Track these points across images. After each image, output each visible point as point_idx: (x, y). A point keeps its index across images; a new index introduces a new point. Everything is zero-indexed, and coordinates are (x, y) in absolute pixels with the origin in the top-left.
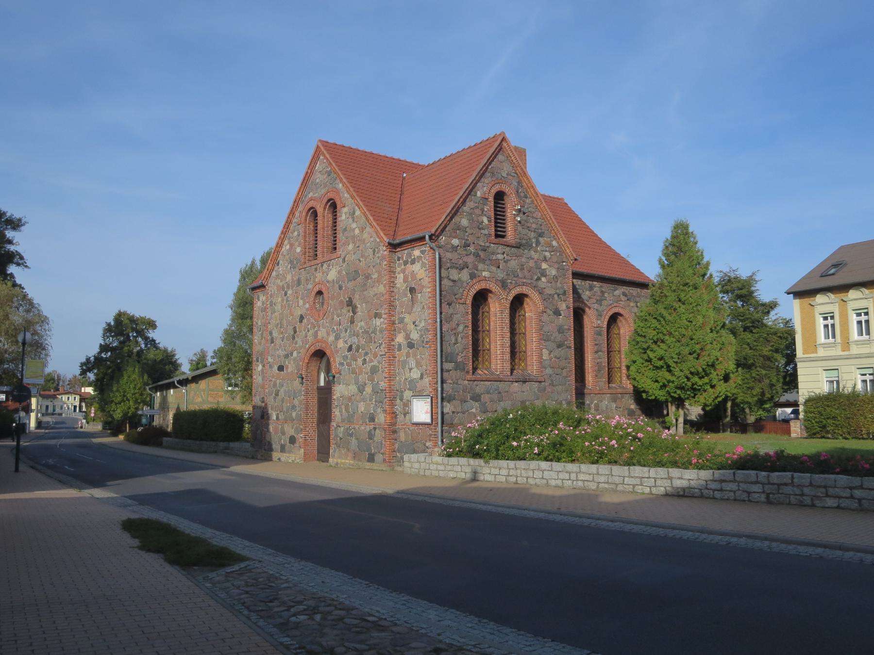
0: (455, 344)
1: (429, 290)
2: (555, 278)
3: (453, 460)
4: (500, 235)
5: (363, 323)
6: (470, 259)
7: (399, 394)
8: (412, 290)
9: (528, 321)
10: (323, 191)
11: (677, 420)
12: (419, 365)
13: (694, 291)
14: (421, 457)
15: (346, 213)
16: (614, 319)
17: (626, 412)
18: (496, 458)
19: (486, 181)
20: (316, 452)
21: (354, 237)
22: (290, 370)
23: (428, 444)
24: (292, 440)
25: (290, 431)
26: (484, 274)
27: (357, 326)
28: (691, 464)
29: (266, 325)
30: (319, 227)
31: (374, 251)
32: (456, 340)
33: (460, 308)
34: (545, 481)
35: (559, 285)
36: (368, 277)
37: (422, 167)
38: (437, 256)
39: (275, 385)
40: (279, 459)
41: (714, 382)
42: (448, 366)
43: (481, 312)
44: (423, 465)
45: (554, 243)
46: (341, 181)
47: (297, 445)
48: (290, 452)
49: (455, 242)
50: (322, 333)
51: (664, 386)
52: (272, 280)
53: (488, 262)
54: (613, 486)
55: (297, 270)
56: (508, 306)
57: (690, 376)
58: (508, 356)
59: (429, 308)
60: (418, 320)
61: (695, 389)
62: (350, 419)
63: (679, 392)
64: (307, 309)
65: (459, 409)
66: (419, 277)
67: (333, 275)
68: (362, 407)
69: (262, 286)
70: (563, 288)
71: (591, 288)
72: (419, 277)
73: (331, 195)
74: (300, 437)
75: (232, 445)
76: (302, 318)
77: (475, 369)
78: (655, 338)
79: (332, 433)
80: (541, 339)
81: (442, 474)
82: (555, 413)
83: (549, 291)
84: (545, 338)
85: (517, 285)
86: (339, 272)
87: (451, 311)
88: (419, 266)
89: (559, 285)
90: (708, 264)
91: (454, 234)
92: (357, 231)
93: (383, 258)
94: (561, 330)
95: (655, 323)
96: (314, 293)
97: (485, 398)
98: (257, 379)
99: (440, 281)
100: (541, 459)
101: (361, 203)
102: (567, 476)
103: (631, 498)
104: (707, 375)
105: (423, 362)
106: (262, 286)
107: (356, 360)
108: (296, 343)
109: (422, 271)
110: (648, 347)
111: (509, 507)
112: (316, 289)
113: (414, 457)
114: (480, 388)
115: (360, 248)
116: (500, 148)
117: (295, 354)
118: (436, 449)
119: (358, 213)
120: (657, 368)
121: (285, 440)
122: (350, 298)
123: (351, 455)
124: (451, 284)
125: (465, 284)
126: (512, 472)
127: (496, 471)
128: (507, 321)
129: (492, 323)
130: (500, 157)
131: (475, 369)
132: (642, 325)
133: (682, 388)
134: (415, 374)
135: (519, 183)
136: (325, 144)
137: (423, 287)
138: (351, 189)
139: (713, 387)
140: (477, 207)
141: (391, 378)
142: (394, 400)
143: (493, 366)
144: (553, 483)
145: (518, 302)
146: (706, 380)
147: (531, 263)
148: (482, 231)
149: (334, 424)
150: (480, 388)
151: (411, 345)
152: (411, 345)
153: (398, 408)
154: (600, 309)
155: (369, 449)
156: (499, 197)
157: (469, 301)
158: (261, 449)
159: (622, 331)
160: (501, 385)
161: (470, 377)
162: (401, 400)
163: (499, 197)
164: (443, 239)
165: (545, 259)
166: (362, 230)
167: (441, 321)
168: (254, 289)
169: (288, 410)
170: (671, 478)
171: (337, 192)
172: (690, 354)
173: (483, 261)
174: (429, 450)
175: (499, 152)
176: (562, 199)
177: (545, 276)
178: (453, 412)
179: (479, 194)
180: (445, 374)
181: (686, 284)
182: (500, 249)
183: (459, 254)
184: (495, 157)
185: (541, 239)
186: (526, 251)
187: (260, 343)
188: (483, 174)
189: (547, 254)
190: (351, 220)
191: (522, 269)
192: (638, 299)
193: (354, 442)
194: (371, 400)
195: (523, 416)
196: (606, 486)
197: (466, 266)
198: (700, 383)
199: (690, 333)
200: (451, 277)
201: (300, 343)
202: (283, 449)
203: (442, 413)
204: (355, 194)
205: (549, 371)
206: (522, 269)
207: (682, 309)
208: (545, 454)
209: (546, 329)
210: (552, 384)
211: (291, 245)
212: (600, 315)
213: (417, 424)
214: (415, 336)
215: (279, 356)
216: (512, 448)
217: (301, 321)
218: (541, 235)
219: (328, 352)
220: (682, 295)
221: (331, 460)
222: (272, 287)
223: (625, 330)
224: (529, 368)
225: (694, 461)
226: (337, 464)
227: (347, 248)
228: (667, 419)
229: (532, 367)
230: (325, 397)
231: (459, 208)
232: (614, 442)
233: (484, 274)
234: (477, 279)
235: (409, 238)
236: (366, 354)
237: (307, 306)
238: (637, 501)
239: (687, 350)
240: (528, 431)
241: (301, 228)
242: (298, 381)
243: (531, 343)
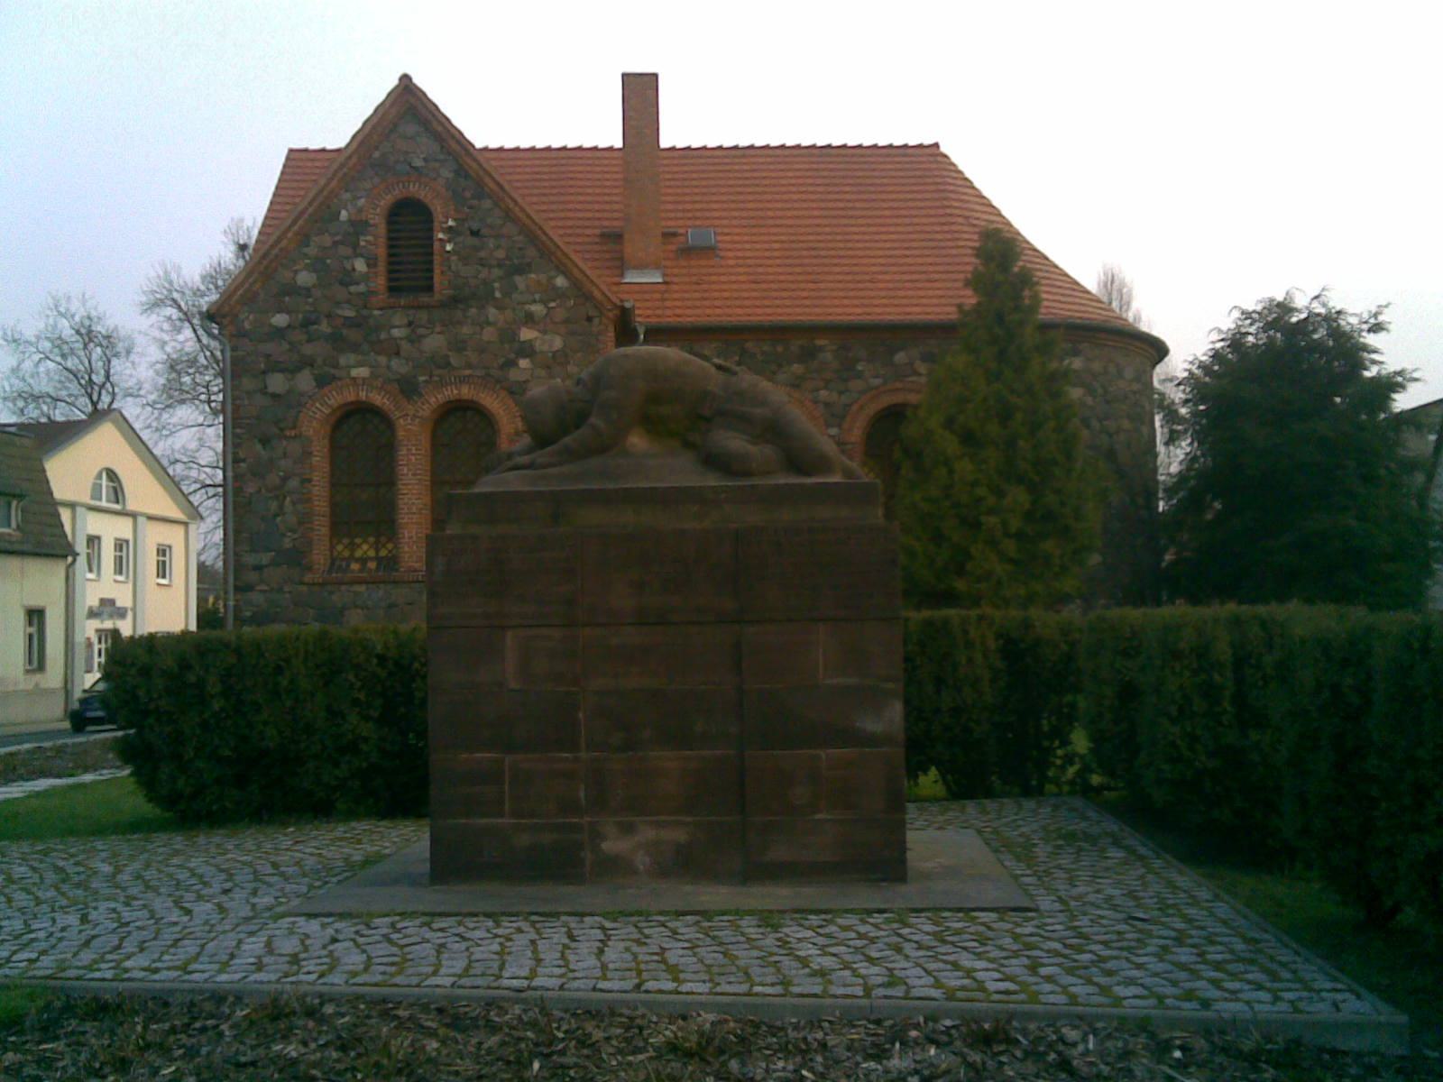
0: (276, 515)
2: (560, 358)
26: (355, 372)
32: (281, 507)
45: (560, 281)
49: (280, 320)
53: (365, 347)
147: (489, 334)
148: (353, 289)
165: (530, 319)
173: (355, 348)
179: (344, 215)
182: (399, 318)
183: (290, 343)
186: (473, 311)
189: (537, 309)
197: (309, 363)
200: (270, 390)
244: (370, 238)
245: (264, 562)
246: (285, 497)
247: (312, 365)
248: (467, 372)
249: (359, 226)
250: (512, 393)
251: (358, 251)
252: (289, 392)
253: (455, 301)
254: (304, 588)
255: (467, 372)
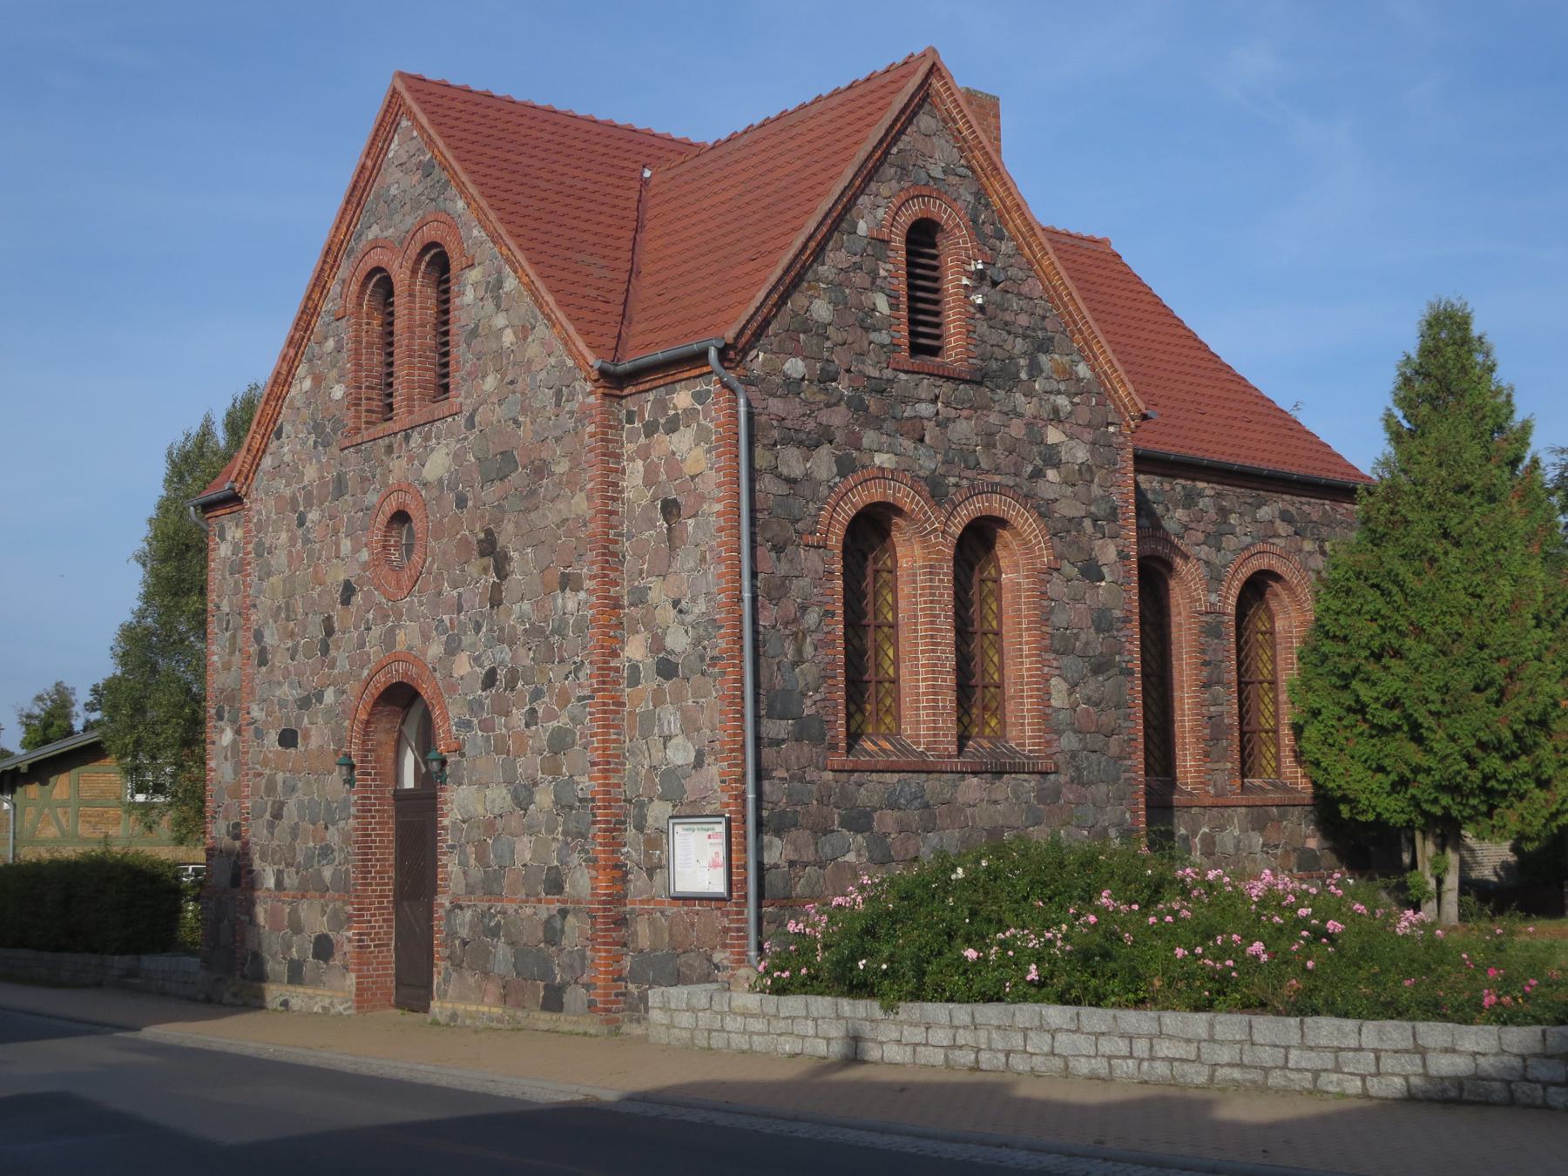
0: (795, 664)
1: (718, 507)
2: (1086, 471)
3: (793, 1004)
4: (924, 343)
5: (526, 606)
6: (837, 418)
7: (632, 811)
8: (670, 509)
9: (1007, 597)
10: (410, 221)
11: (1440, 882)
12: (690, 726)
13: (1486, 507)
14: (699, 994)
15: (475, 285)
16: (1256, 588)
17: (1293, 859)
18: (918, 995)
19: (885, 190)
20: (391, 983)
21: (499, 354)
22: (314, 743)
23: (718, 957)
24: (324, 948)
25: (316, 921)
26: (879, 459)
27: (509, 612)
28: (1479, 1007)
29: (243, 612)
30: (399, 325)
31: (559, 394)
32: (799, 651)
33: (811, 560)
34: (1058, 1063)
35: (1096, 491)
36: (540, 470)
37: (698, 150)
38: (742, 409)
39: (271, 788)
40: (285, 1004)
41: (1549, 771)
42: (776, 728)
43: (869, 571)
44: (705, 1019)
45: (1083, 370)
46: (463, 192)
47: (337, 961)
48: (317, 982)
49: (795, 367)
50: (407, 636)
51: (1402, 783)
52: (260, 481)
53: (889, 425)
54: (1256, 1075)
55: (335, 450)
56: (949, 552)
57: (1477, 753)
58: (949, 699)
59: (720, 560)
60: (689, 593)
61: (1490, 792)
62: (490, 886)
63: (1445, 800)
64: (365, 566)
65: (809, 855)
66: (689, 468)
67: (437, 464)
68: (525, 850)
69: (234, 499)
70: (1106, 498)
71: (1190, 500)
72: (689, 468)
73: (430, 233)
74: (346, 939)
75: (149, 962)
76: (348, 590)
77: (853, 737)
78: (1375, 644)
79: (439, 925)
80: (1046, 649)
81: (759, 1043)
82: (1088, 863)
83: (1066, 509)
84: (1057, 645)
85: (975, 491)
86: (457, 457)
87: (783, 568)
88: (690, 441)
89: (1096, 491)
90: (1526, 428)
91: (790, 345)
92: (508, 338)
93: (583, 415)
94: (1102, 622)
95: (1375, 601)
96: (382, 519)
97: (886, 821)
98: (220, 770)
99: (752, 481)
100: (1046, 999)
101: (520, 256)
102: (1122, 1046)
103: (1308, 1108)
104: (1526, 750)
105: (703, 719)
106: (234, 499)
107: (507, 714)
108: (332, 666)
109: (699, 452)
110: (1356, 671)
111: (953, 1140)
112: (390, 507)
113: (678, 994)
114: (870, 790)
115: (519, 386)
116: (922, 98)
117: (329, 696)
118: (742, 972)
119: (511, 283)
120: (1382, 730)
121: (302, 947)
122: (489, 532)
123: (493, 989)
124: (784, 489)
125: (824, 491)
126: (963, 1037)
127: (918, 1035)
128: (948, 597)
129: (902, 604)
130: (925, 121)
131: (853, 737)
132: (1336, 605)
133: (1453, 789)
134: (680, 754)
135: (980, 194)
136: (416, 83)
137: (702, 498)
138: (492, 216)
139: (1543, 784)
140: (857, 267)
141: (609, 764)
142: (619, 828)
143: (907, 730)
144: (1083, 1067)
145: (977, 543)
146: (1524, 764)
147: (1017, 429)
148: (873, 336)
149: (443, 900)
150: (870, 790)
151: (667, 669)
152: (667, 669)
153: (632, 851)
154: (1217, 559)
155: (547, 974)
156: (923, 235)
157: (836, 540)
158: (233, 976)
159: (1279, 625)
160: (931, 784)
161: (837, 760)
162: (640, 828)
163: (923, 235)
164: (759, 359)
165: (1056, 417)
166: (524, 332)
167: (754, 599)
168: (208, 507)
169: (309, 858)
170: (1422, 1051)
171: (451, 223)
172: (1477, 689)
173: (876, 423)
174: (720, 975)
175: (920, 106)
176: (1104, 242)
177: (1057, 465)
178: (792, 864)
179: (862, 228)
180: (765, 751)
181: (1464, 488)
182: (926, 387)
183: (806, 403)
184: (910, 121)
185: (1043, 359)
186: (1001, 393)
187: (227, 666)
188: (876, 169)
189: (1062, 401)
190: (489, 305)
191: (989, 446)
192: (1325, 531)
193: (502, 952)
194: (551, 831)
195: (994, 874)
196: (1237, 1074)
198: (1507, 774)
199: (1477, 630)
200: (785, 472)
201: (343, 664)
202: (296, 975)
203: (760, 865)
204: (502, 230)
205: (1068, 741)
206: (989, 446)
207: (1454, 559)
208: (1060, 982)
209: (1060, 619)
210: (1078, 780)
211: (318, 380)
212: (1215, 578)
213: (687, 899)
214: (678, 641)
215: (282, 704)
216: (964, 967)
217: (346, 601)
218: (1045, 346)
219: (426, 691)
220: (1453, 520)
221: (435, 1005)
222: (260, 504)
223: (1290, 619)
224: (1012, 732)
225: (1489, 999)
226: (454, 1016)
227: (480, 386)
228: (1412, 878)
229: (1022, 730)
230: (416, 820)
231: (805, 268)
232: (1258, 946)
233: (879, 459)
234: (860, 475)
235: (660, 355)
236: (537, 695)
237: (365, 555)
238: (1323, 1119)
239: (1468, 678)
240: (1008, 917)
241: (346, 329)
242: (337, 776)
243: (1019, 659)
244: (890, 267)
245: (783, 735)
246: (804, 637)
247: (831, 442)
248: (997, 479)
249: (880, 243)
250: (1041, 515)
251: (878, 282)
252: (808, 476)
253: (977, 379)
254: (829, 776)
255: (997, 479)
